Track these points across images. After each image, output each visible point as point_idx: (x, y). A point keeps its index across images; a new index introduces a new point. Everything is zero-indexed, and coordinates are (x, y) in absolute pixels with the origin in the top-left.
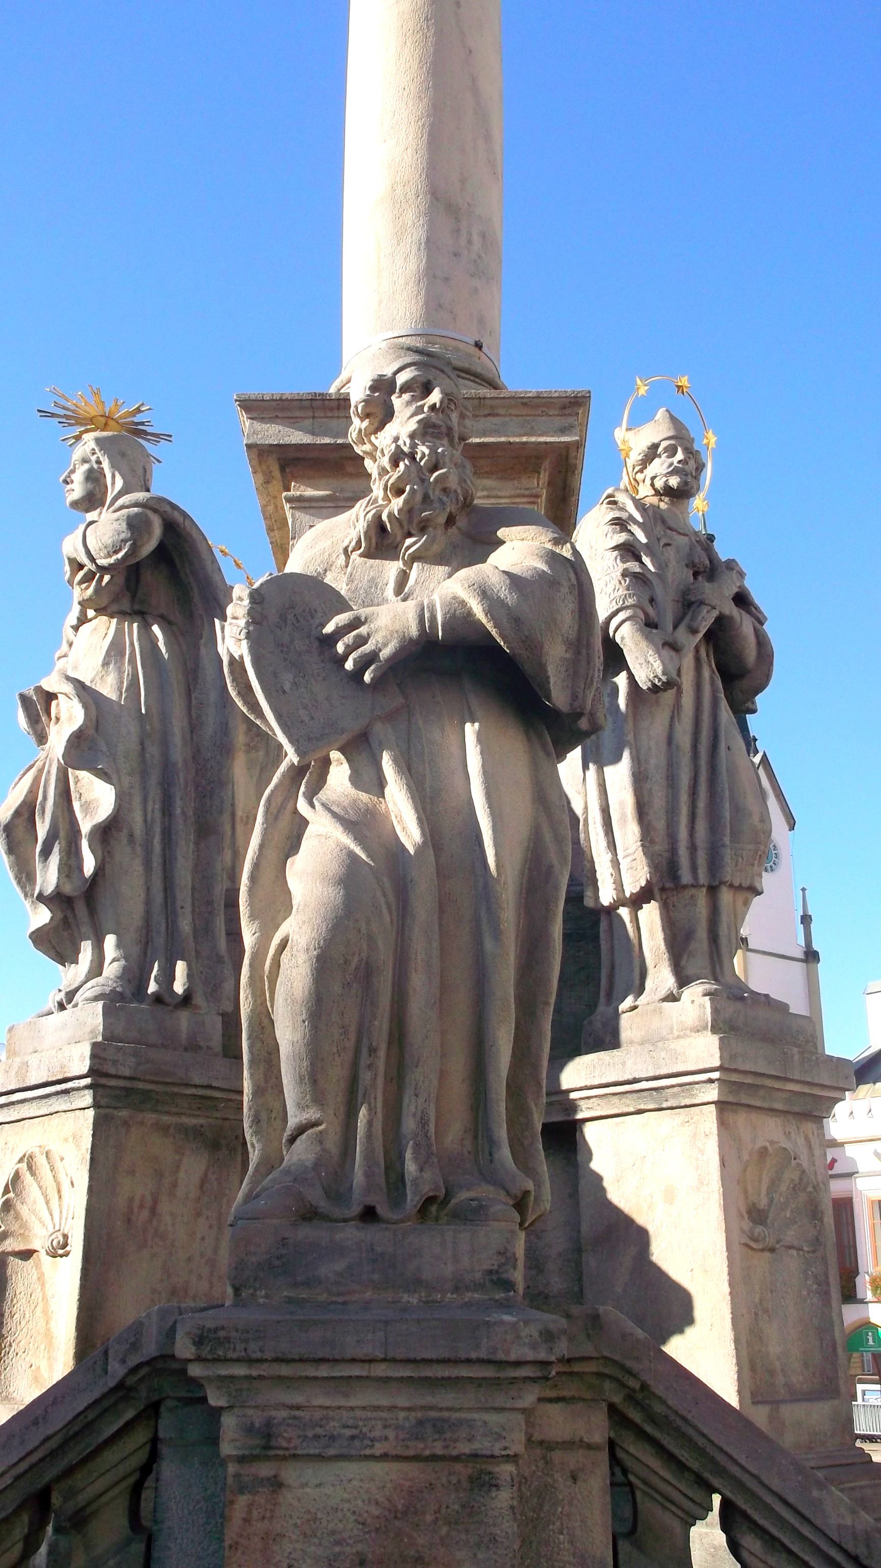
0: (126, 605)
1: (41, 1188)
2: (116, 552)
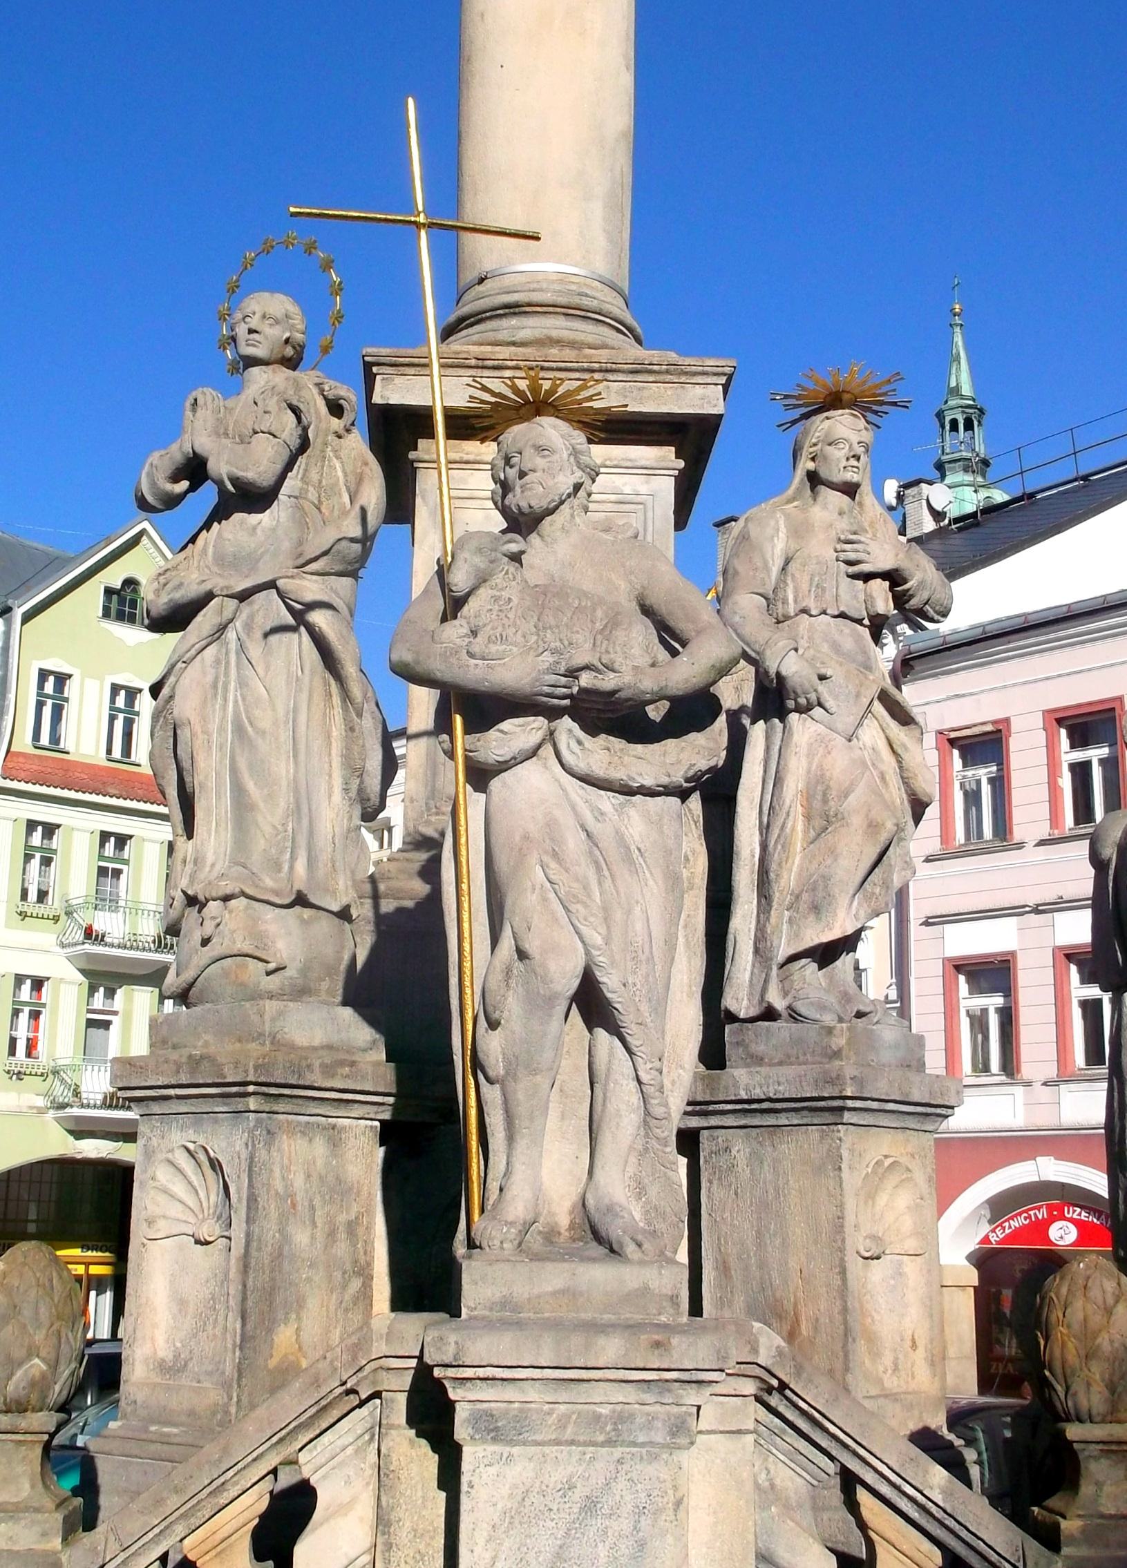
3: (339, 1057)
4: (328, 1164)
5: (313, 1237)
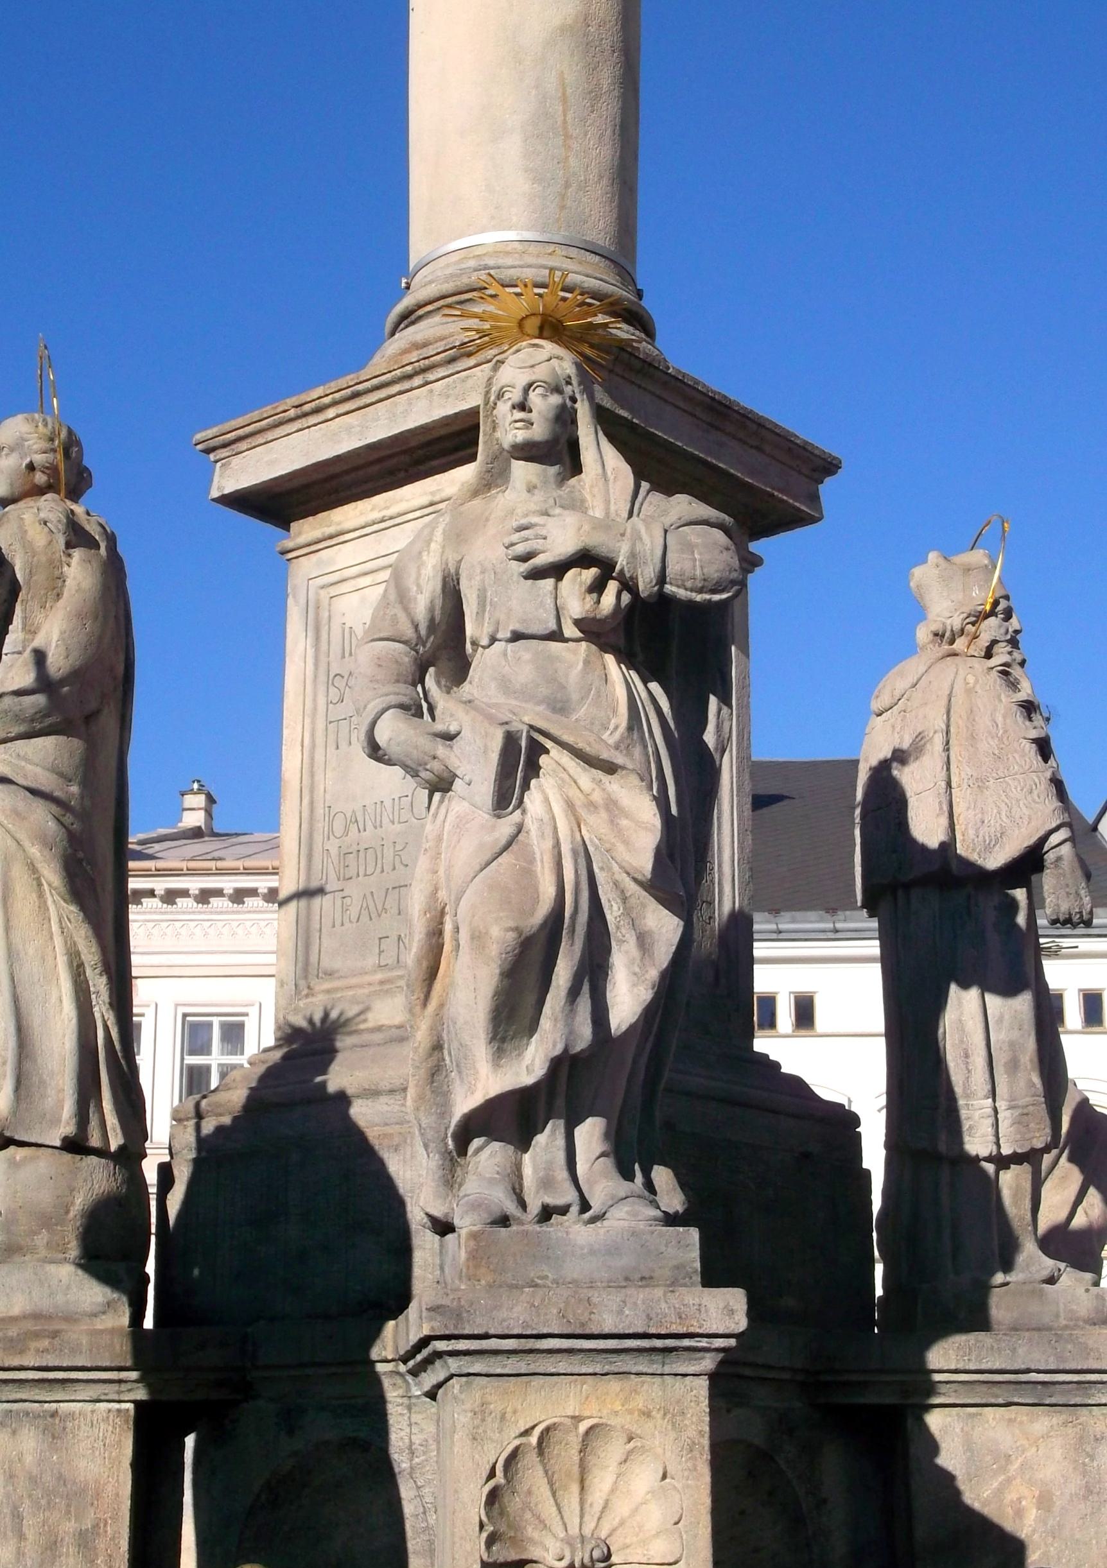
0: (622, 643)
1: (546, 1472)
2: (713, 591)
3: (45, 1324)
4: (40, 1462)
5: (20, 1554)
